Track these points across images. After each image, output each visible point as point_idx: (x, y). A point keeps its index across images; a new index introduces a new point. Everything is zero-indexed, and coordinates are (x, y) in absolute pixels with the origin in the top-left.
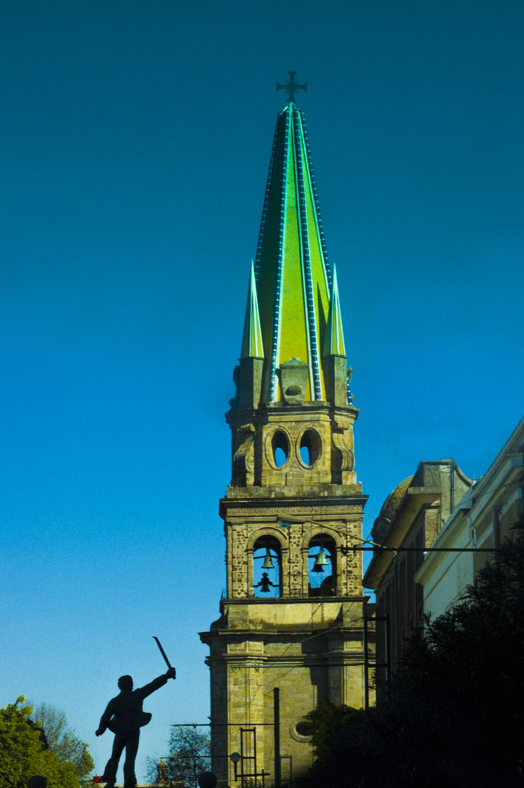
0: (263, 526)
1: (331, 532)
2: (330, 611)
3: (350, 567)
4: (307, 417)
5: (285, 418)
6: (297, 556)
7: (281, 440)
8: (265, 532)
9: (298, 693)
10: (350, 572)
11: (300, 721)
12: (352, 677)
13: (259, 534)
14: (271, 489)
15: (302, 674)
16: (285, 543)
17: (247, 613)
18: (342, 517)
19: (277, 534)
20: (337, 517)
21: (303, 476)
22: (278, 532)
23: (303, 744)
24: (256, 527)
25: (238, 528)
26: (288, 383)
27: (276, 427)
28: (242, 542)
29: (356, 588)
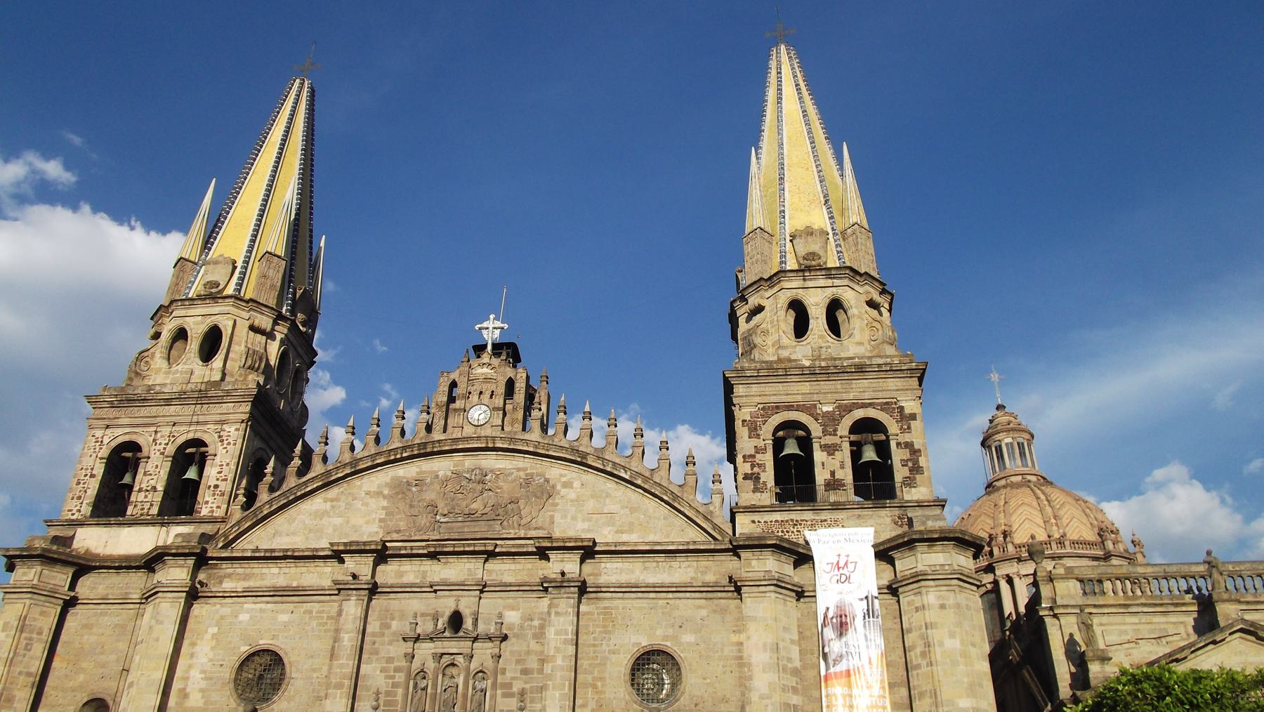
0: (127, 430)
2: (172, 534)
4: (216, 310)
5: (191, 312)
7: (181, 335)
8: (127, 438)
10: (216, 486)
12: (162, 623)
14: (150, 388)
16: (145, 452)
17: (73, 537)
18: (224, 417)
19: (141, 441)
20: (218, 418)
25: (99, 433)
26: (210, 278)
29: (218, 507)
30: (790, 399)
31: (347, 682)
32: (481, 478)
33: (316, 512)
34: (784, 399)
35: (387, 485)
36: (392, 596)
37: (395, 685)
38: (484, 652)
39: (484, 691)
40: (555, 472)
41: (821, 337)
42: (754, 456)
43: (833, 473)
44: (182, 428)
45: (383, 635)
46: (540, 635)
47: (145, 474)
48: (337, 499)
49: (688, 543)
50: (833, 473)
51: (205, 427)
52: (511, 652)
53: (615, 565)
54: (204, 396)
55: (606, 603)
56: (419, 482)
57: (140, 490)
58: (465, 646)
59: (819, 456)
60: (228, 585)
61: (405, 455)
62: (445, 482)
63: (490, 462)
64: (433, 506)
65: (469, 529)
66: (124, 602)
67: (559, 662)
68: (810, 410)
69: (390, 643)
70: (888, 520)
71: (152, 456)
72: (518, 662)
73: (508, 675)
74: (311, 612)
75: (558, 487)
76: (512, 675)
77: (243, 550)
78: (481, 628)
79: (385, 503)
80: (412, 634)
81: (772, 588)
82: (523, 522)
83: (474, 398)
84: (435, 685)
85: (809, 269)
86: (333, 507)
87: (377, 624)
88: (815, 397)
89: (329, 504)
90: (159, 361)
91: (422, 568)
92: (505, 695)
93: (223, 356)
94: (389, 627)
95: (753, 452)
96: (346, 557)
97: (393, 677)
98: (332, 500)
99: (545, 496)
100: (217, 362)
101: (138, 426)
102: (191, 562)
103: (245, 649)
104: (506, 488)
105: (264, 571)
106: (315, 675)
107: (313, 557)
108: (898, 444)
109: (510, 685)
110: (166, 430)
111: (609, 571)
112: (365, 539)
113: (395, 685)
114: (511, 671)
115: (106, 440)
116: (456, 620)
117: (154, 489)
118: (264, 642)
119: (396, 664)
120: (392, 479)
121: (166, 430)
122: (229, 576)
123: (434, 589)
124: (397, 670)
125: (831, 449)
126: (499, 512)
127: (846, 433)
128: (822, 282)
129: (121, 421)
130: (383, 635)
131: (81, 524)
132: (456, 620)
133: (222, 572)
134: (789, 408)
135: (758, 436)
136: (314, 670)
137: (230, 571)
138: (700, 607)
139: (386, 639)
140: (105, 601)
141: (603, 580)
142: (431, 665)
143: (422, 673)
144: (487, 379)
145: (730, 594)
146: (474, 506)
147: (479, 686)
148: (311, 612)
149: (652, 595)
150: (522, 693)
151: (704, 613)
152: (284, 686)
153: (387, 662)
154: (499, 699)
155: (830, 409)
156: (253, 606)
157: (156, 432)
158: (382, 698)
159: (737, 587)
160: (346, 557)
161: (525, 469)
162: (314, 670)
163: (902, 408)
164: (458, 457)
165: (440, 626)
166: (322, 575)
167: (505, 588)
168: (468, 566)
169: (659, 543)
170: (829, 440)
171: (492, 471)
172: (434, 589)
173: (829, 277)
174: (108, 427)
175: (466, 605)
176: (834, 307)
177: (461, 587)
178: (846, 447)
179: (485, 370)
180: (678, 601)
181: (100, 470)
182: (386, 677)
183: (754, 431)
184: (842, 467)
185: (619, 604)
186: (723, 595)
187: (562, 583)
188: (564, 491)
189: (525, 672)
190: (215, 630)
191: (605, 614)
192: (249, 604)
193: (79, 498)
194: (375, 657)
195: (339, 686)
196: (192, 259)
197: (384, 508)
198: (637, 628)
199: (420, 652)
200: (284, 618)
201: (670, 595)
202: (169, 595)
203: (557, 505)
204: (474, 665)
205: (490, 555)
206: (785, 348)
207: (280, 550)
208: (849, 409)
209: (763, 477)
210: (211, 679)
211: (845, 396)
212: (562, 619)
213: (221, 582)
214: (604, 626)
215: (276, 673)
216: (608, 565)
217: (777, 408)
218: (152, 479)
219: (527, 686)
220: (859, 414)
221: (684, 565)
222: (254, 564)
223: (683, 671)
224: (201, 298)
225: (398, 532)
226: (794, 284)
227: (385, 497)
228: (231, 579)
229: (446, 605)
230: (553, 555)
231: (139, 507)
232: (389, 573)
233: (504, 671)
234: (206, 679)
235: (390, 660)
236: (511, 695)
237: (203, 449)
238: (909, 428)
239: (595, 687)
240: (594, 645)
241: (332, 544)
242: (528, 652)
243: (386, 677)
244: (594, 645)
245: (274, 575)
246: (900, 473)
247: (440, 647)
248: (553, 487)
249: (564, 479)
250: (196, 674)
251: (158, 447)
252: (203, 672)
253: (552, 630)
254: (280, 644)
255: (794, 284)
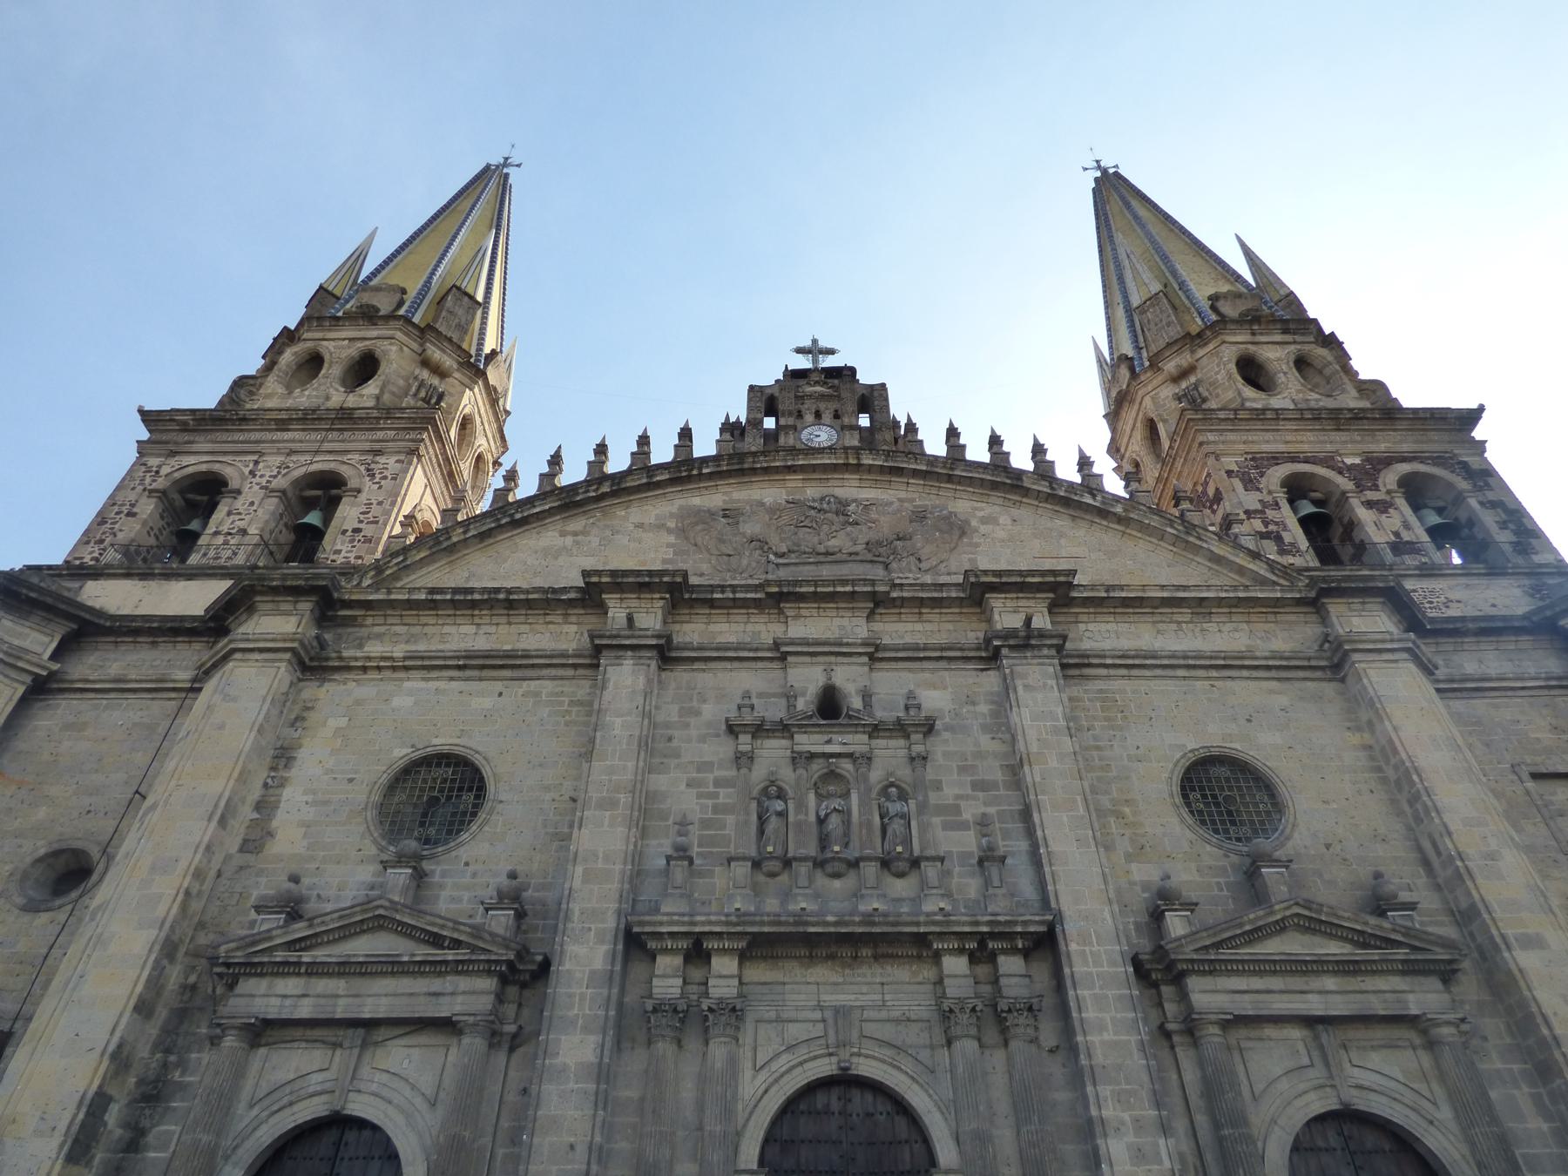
1: (345, 471)
3: (361, 522)
4: (375, 333)
6: (252, 503)
8: (204, 468)
9: (97, 771)
10: (357, 531)
11: (56, 846)
12: (235, 699)
13: (190, 470)
15: (135, 724)
18: (377, 446)
19: (227, 471)
20: (367, 446)
21: (328, 398)
22: (233, 470)
23: (27, 917)
24: (192, 459)
27: (309, 344)
28: (148, 480)
30: (1291, 448)
31: (623, 798)
32: (841, 507)
33: (546, 552)
34: (1282, 448)
35: (672, 515)
36: (696, 666)
37: (716, 809)
38: (889, 756)
39: (906, 817)
40: (963, 505)
41: (1299, 391)
42: (1262, 512)
43: (1397, 534)
44: (303, 458)
45: (687, 726)
46: (1001, 721)
47: (229, 513)
48: (584, 533)
49: (1235, 588)
50: (1397, 534)
51: (345, 459)
52: (945, 754)
53: (1103, 627)
54: (345, 419)
55: (1100, 685)
56: (726, 513)
57: (217, 533)
58: (857, 742)
59: (1364, 515)
60: (374, 649)
61: (705, 471)
62: (773, 511)
63: (850, 489)
64: (760, 543)
65: (826, 572)
66: (158, 689)
67: (1053, 763)
68: (1328, 461)
69: (702, 739)
70: (1517, 592)
71: (246, 490)
72: (963, 770)
73: (949, 793)
74: (537, 694)
75: (974, 523)
76: (957, 791)
77: (411, 590)
78: (880, 714)
79: (672, 539)
80: (748, 718)
81: (1405, 656)
82: (924, 566)
83: (809, 418)
84: (801, 806)
85: (1257, 319)
86: (577, 543)
87: (675, 708)
88: (1329, 447)
89: (569, 540)
90: (272, 384)
91: (750, 627)
92: (947, 826)
93: (380, 383)
94: (698, 713)
95: (1259, 507)
96: (611, 600)
97: (715, 796)
98: (575, 534)
99: (957, 533)
100: (371, 388)
101: (225, 453)
102: (306, 606)
103: (401, 753)
104: (885, 526)
105: (447, 629)
106: (548, 797)
107: (546, 602)
108: (1482, 504)
109: (956, 810)
110: (276, 460)
111: (1098, 635)
112: (657, 566)
113: (716, 809)
114: (952, 788)
115: (165, 470)
116: (830, 706)
117: (243, 532)
118: (443, 740)
119: (718, 773)
120: (681, 508)
121: (276, 460)
122: (379, 636)
123: (780, 654)
124: (718, 783)
125: (1382, 507)
126: (880, 552)
127: (1394, 487)
128: (1278, 338)
129: (195, 447)
130: (687, 726)
131: (96, 572)
132: (830, 706)
133: (364, 632)
134: (1293, 459)
135: (1258, 489)
136: (547, 789)
137: (382, 629)
138: (1271, 692)
139: (694, 733)
140: (121, 688)
141: (1086, 645)
142: (787, 775)
143: (773, 791)
144: (822, 397)
145: (1319, 674)
146: (833, 542)
147: (895, 807)
148: (537, 694)
149: (1181, 672)
150: (983, 823)
151: (1284, 700)
152: (482, 816)
153: (699, 771)
154: (940, 834)
155: (1357, 461)
156: (422, 684)
157: (256, 463)
158: (695, 831)
159: (1335, 662)
160: (611, 600)
161: (913, 500)
162: (547, 789)
163: (1465, 463)
164: (794, 481)
165: (801, 704)
166: (567, 635)
167: (914, 655)
168: (837, 621)
169: (1185, 588)
170: (1371, 495)
171: (855, 501)
172: (780, 654)
173: (1285, 331)
174: (173, 454)
175: (849, 678)
176: (1301, 363)
177: (835, 650)
178: (1401, 502)
179: (818, 388)
180: (1229, 683)
181: (148, 507)
182: (700, 796)
183: (1250, 484)
184: (1407, 526)
185: (1123, 687)
186: (1308, 674)
187: (1025, 640)
188: (983, 529)
189: (980, 786)
190: (343, 722)
191: (1104, 700)
192: (415, 684)
193: (101, 541)
194: (673, 762)
195: (612, 804)
196: (337, 292)
197: (668, 545)
198: (1172, 725)
199: (764, 753)
200: (487, 703)
201: (1214, 673)
202: (257, 656)
203: (977, 545)
204: (876, 775)
205: (878, 603)
206: (1254, 400)
207: (484, 590)
208: (1388, 461)
209: (1287, 537)
210: (326, 803)
211: (1373, 447)
212: (1040, 696)
213: (361, 646)
214: (1107, 719)
215: (468, 798)
216: (1091, 627)
217: (1275, 459)
218: (245, 521)
219: (991, 810)
220: (1405, 468)
221: (1229, 626)
222: (427, 617)
223: (1282, 790)
224: (350, 317)
225: (702, 575)
226: (1239, 338)
227: (669, 531)
228: (383, 640)
229: (808, 679)
230: (997, 602)
231: (212, 554)
232: (693, 631)
233: (938, 786)
234: (315, 803)
235: (704, 767)
236: (963, 826)
237: (334, 492)
238: (1487, 484)
239: (1119, 815)
240: (1098, 748)
241: (586, 574)
242: (979, 755)
243: (700, 796)
244: (1098, 748)
245: (464, 636)
246: (1504, 538)
247: (809, 742)
248: (967, 522)
249: (981, 514)
250: (293, 798)
251: (257, 479)
252: (305, 793)
253: (1025, 712)
254: (478, 743)
255: (1239, 338)
